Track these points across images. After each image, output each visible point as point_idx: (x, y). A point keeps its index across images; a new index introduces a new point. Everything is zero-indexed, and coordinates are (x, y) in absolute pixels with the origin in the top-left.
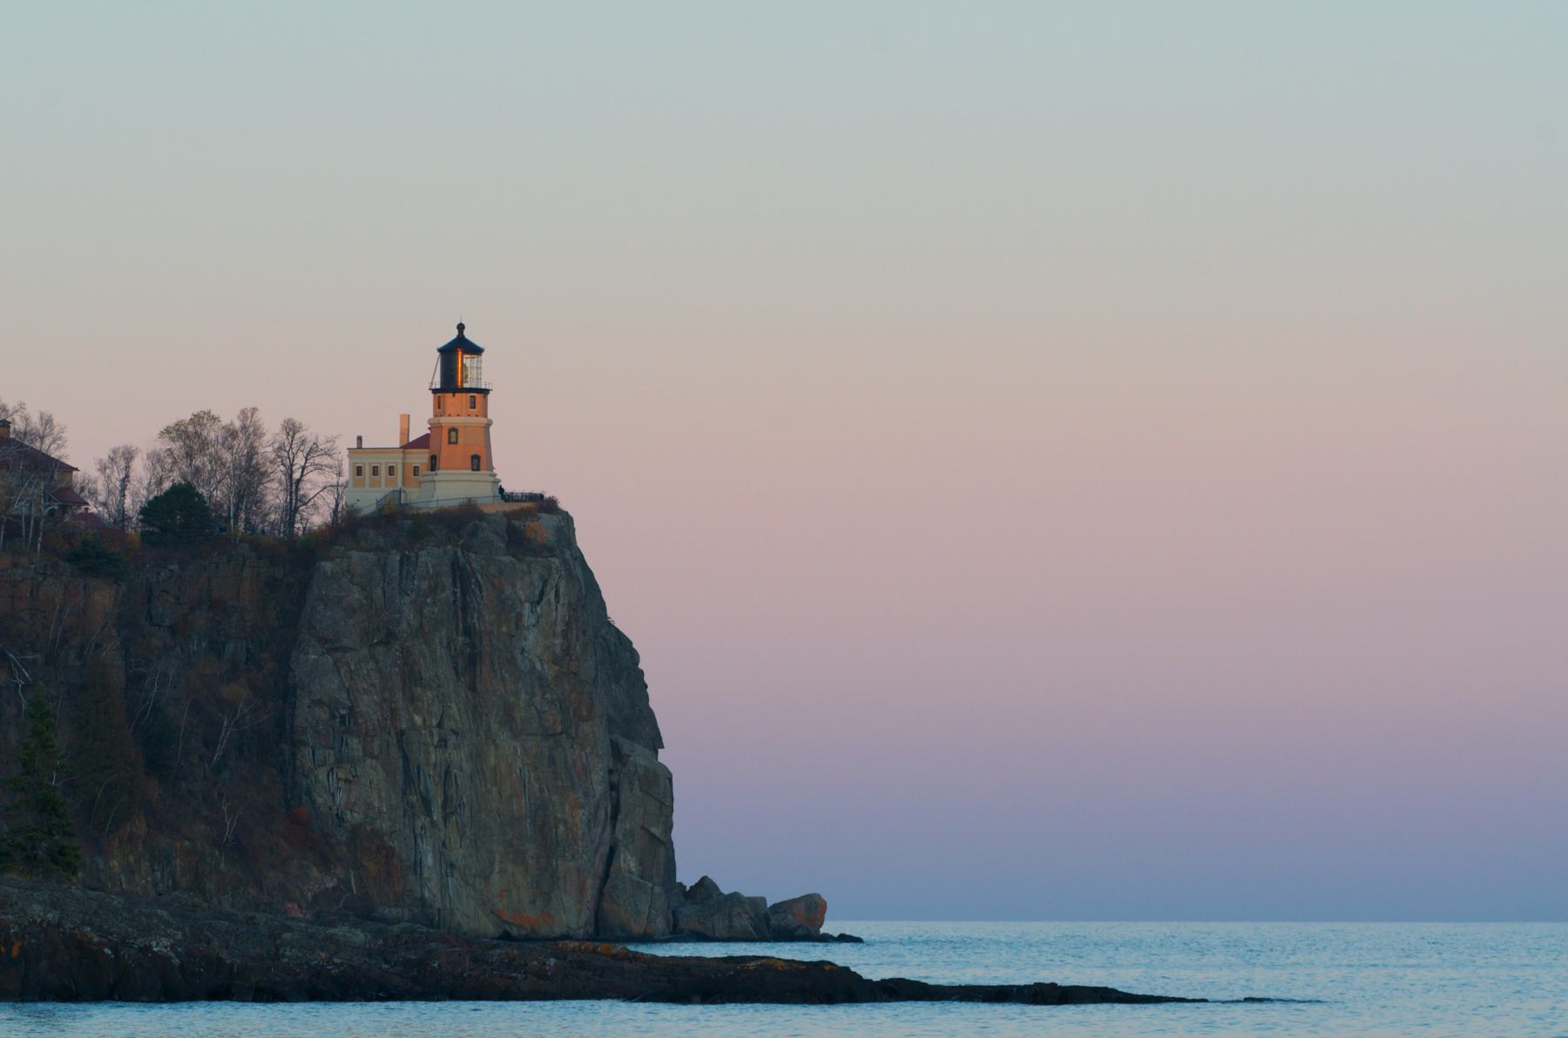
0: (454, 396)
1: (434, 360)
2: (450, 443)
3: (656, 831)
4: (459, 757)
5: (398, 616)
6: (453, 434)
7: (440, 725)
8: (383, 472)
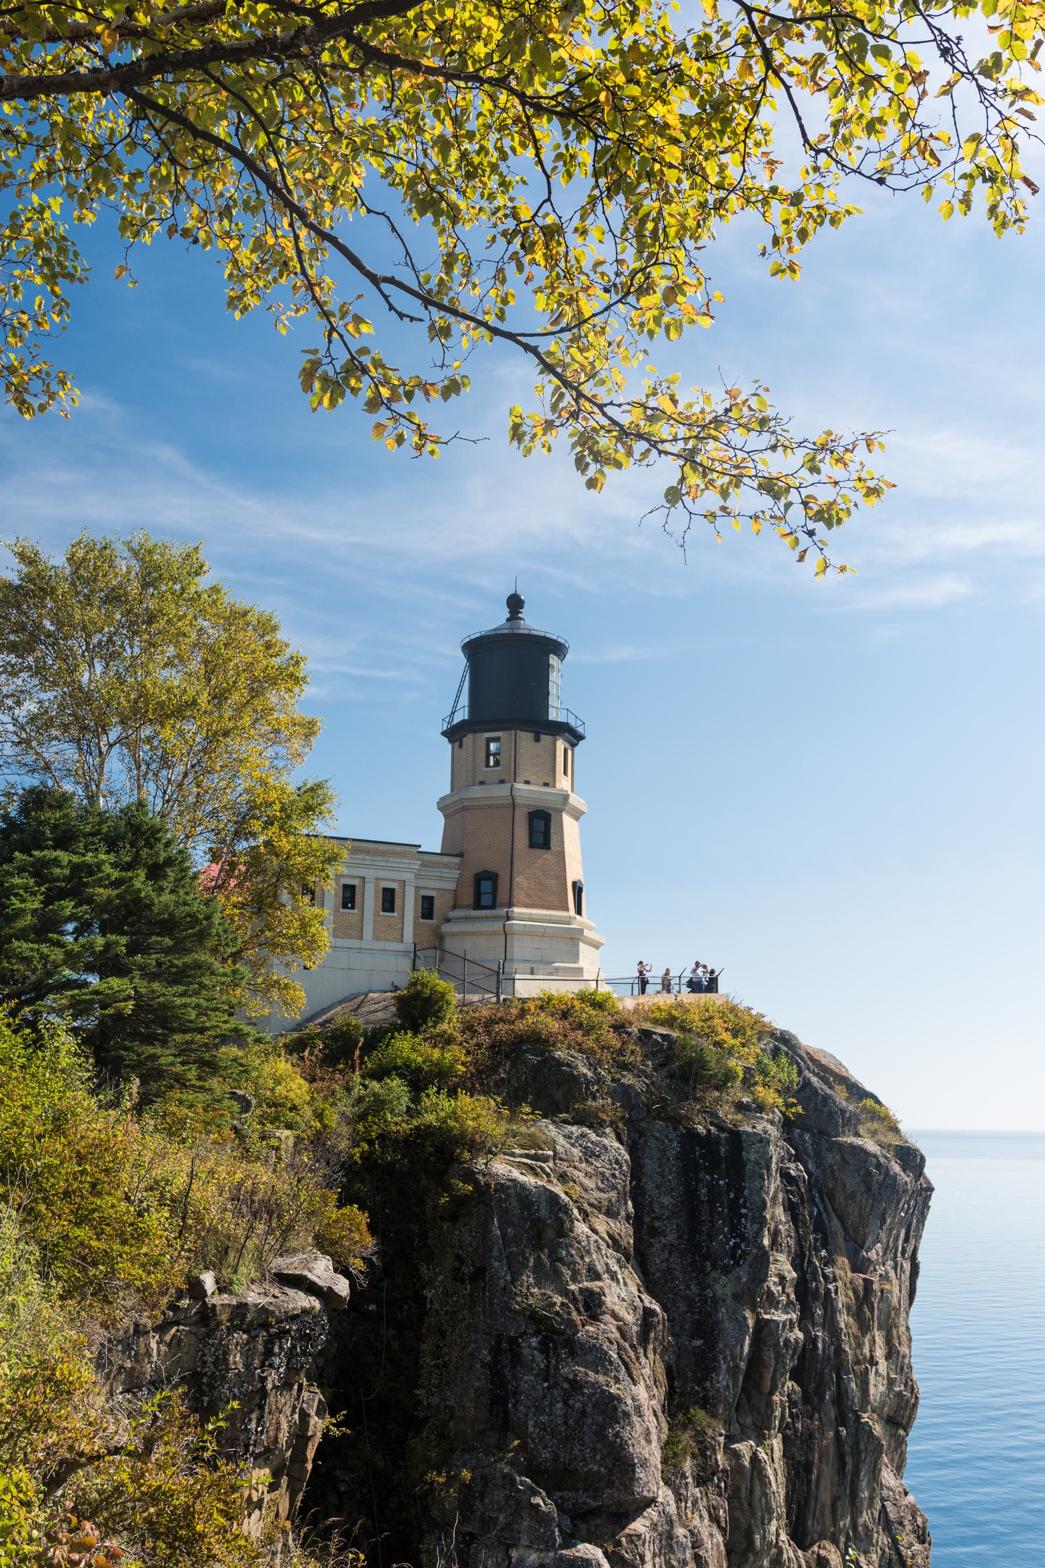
0: (537, 740)
1: (460, 661)
2: (532, 845)
5: (698, 1343)
6: (540, 825)
8: (370, 900)
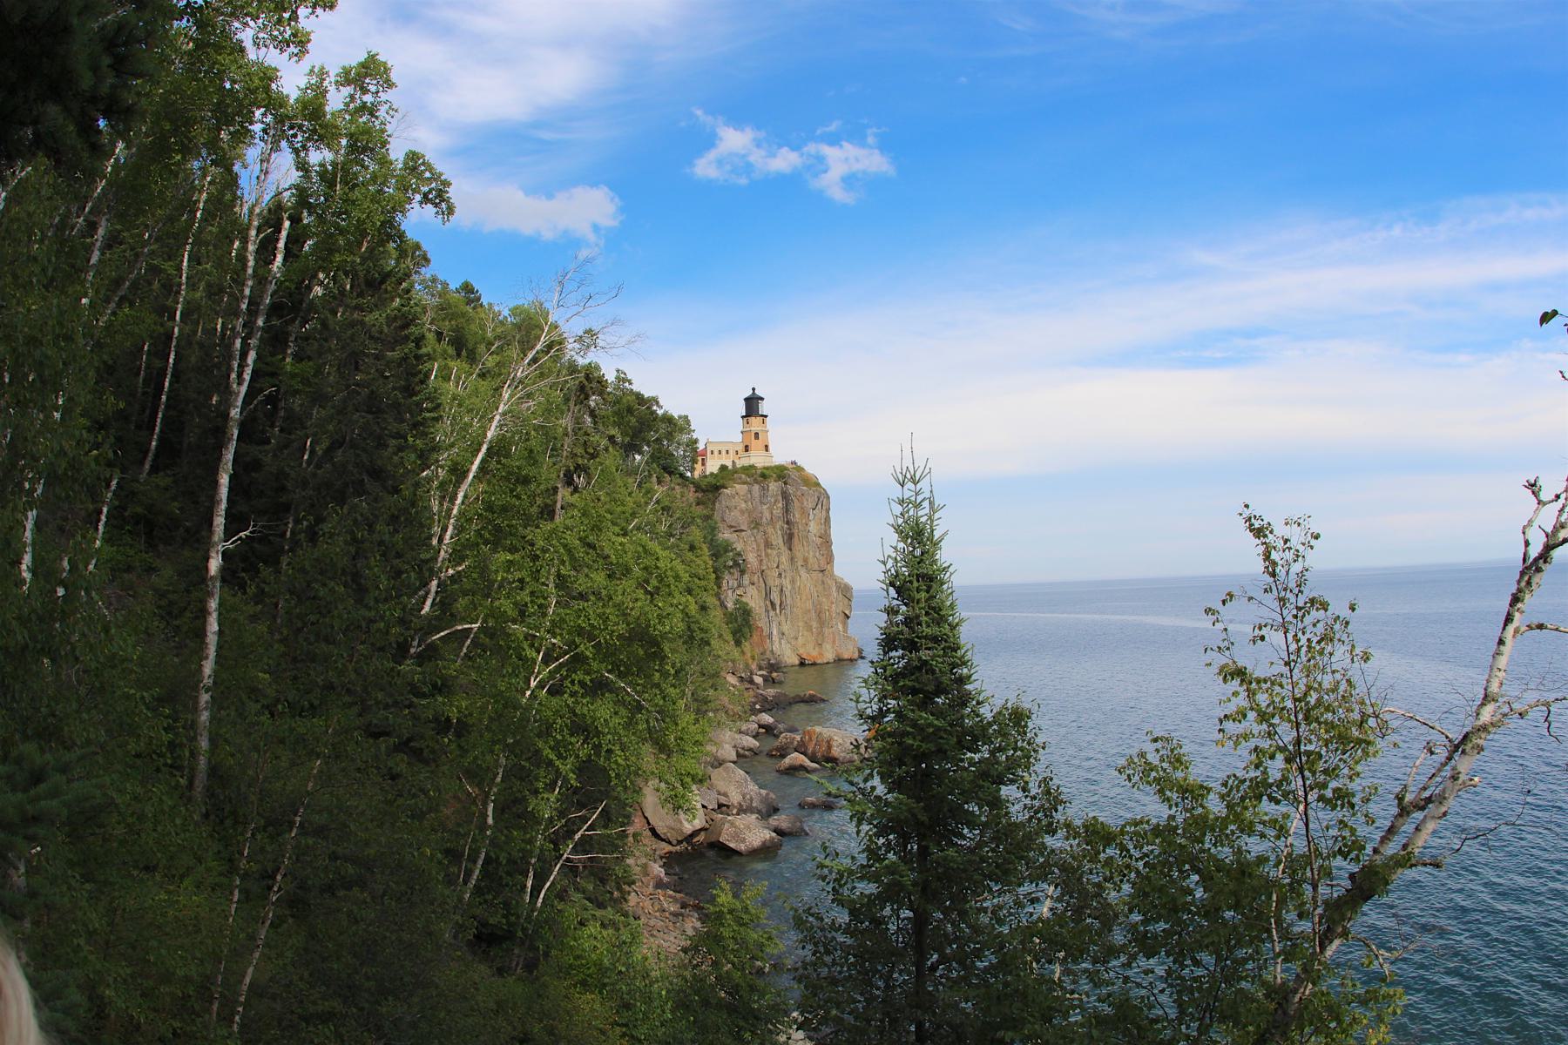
1: (742, 405)
3: (847, 612)
4: (786, 583)
7: (778, 567)
8: (724, 452)
